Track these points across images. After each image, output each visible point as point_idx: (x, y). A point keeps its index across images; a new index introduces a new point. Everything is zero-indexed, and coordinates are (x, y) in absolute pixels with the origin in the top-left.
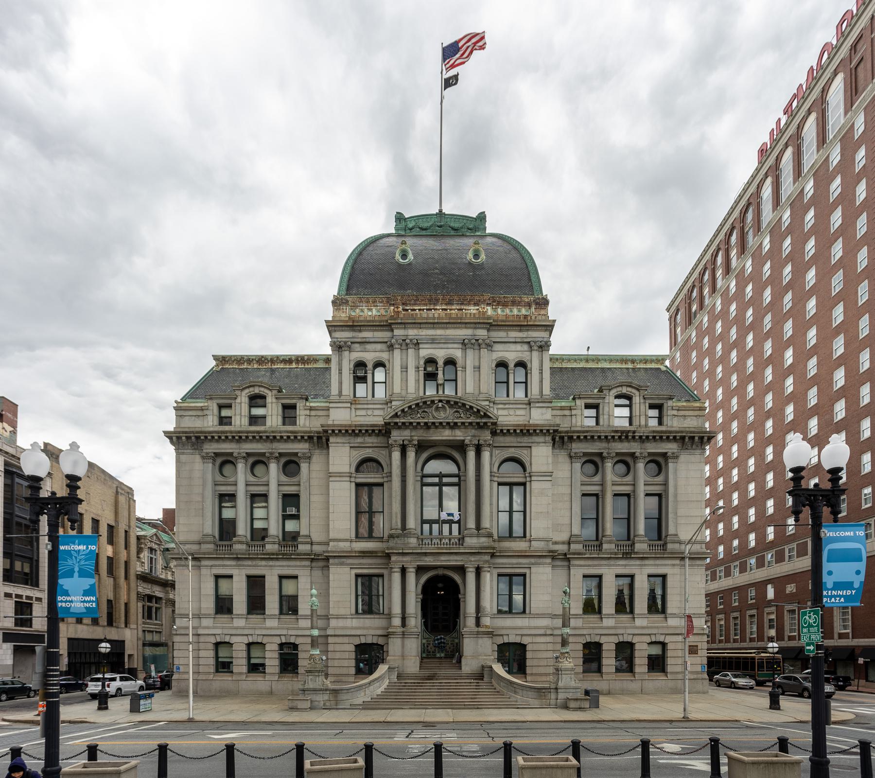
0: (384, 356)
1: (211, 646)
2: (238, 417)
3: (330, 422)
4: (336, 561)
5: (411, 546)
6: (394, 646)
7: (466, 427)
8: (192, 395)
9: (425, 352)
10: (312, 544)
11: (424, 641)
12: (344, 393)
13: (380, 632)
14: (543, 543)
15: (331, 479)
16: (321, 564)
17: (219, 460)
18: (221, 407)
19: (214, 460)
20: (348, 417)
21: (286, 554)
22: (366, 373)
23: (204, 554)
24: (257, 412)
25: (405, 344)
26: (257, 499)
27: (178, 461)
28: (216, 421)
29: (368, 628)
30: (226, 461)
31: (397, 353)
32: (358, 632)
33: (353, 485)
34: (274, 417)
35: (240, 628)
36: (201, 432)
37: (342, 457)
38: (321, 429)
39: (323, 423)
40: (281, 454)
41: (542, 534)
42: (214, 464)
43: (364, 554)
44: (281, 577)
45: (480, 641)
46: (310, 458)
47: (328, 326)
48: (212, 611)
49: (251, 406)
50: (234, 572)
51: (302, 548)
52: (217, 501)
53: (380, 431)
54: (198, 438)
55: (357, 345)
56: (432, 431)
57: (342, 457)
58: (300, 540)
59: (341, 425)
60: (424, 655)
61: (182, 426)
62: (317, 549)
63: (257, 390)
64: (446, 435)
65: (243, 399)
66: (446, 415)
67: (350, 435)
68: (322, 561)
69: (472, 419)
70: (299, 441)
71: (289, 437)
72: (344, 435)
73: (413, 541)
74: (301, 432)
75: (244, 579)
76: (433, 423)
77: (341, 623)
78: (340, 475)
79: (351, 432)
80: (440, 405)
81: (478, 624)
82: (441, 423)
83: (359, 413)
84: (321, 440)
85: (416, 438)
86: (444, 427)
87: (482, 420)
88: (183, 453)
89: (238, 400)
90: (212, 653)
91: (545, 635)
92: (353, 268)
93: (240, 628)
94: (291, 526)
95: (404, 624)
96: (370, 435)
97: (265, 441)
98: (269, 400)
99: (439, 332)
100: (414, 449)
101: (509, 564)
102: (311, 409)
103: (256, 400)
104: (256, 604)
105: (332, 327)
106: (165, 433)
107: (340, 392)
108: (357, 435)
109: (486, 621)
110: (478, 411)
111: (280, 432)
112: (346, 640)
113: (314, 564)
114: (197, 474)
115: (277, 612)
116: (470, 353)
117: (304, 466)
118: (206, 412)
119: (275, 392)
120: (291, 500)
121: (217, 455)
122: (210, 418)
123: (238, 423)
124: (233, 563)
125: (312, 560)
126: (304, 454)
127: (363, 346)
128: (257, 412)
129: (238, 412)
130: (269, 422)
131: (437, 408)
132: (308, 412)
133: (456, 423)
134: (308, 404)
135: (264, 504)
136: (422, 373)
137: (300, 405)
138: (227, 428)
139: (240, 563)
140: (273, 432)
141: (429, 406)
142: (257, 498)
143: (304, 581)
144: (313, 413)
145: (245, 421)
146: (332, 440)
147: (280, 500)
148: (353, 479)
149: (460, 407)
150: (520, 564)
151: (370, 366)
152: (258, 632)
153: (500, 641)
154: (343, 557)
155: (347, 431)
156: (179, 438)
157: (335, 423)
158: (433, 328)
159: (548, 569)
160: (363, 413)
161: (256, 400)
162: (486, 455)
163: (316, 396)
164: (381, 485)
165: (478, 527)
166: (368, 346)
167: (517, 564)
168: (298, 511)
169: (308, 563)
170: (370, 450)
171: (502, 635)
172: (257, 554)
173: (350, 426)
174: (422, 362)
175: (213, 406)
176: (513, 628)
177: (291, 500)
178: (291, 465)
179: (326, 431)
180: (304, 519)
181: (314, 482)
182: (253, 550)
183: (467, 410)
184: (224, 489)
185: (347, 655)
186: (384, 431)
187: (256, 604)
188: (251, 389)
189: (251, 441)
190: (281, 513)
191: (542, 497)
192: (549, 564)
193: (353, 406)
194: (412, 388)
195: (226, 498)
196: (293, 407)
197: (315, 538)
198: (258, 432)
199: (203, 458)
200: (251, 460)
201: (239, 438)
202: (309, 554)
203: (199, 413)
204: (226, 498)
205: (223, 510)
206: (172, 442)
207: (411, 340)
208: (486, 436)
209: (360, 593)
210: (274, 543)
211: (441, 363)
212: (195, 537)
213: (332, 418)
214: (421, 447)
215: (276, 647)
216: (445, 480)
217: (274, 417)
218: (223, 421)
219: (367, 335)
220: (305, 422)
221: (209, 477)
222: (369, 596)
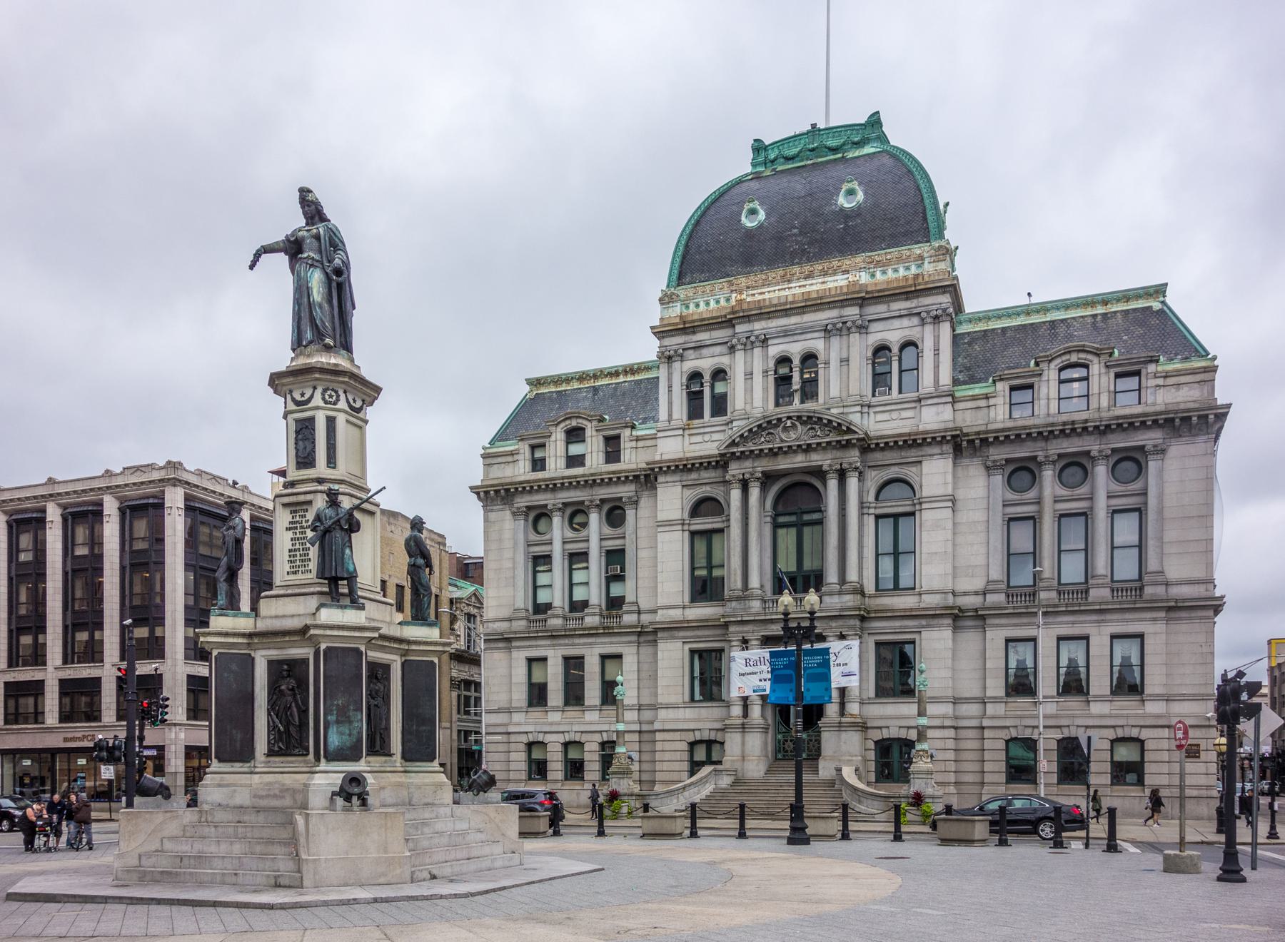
0: (724, 361)
1: (522, 747)
2: (553, 459)
3: (658, 458)
4: (665, 634)
5: (753, 610)
6: (733, 743)
7: (824, 449)
8: (501, 436)
9: (775, 350)
10: (639, 613)
11: (779, 737)
12: (675, 417)
13: (718, 725)
14: (938, 596)
15: (660, 529)
16: (650, 638)
17: (532, 516)
18: (533, 448)
19: (527, 515)
20: (680, 448)
21: (608, 628)
22: (702, 385)
23: (515, 633)
24: (575, 449)
25: (749, 344)
26: (575, 559)
27: (486, 520)
28: (528, 465)
29: (703, 719)
30: (539, 516)
31: (740, 355)
32: (692, 726)
33: (687, 534)
34: (594, 454)
35: (556, 724)
36: (511, 484)
37: (672, 500)
38: (644, 466)
39: (649, 459)
40: (603, 501)
41: (937, 584)
42: (526, 520)
43: (703, 624)
44: (604, 658)
45: (844, 735)
46: (636, 502)
47: (654, 333)
48: (524, 704)
49: (568, 443)
50: (549, 653)
51: (629, 619)
52: (530, 564)
53: (717, 462)
54: (507, 490)
55: (691, 352)
56: (780, 457)
57: (672, 500)
58: (625, 608)
59: (670, 461)
60: (780, 756)
61: (491, 476)
62: (646, 618)
63: (574, 423)
64: (798, 461)
65: (559, 435)
66: (798, 435)
67: (682, 471)
68: (648, 635)
69: (833, 437)
70: (624, 482)
71: (610, 479)
72: (674, 472)
73: (756, 605)
74: (625, 471)
75: (560, 661)
76: (780, 448)
77: (671, 714)
78: (669, 523)
79: (683, 468)
80: (789, 423)
81: (842, 712)
82: (790, 447)
83: (695, 439)
84: (648, 479)
85: (760, 469)
86: (795, 452)
87: (842, 436)
88: (492, 511)
89: (553, 438)
90: (523, 756)
91: (943, 727)
92: (687, 246)
93: (556, 724)
94: (616, 590)
95: (746, 714)
96: (706, 468)
97: (584, 486)
98: (589, 432)
99: (794, 320)
100: (757, 484)
101: (890, 628)
102: (638, 439)
103: (575, 435)
104: (574, 695)
105: (660, 333)
106: (471, 488)
107: (670, 415)
108: (690, 470)
109: (853, 708)
110: (839, 424)
111: (601, 474)
112: (677, 736)
113: (642, 639)
114: (507, 535)
115: (597, 702)
117: (630, 513)
118: (516, 457)
119: (595, 423)
120: (615, 557)
121: (529, 508)
122: (521, 464)
123: (553, 466)
124: (548, 642)
125: (640, 634)
126: (630, 498)
127: (698, 352)
128: (575, 449)
129: (552, 453)
130: (588, 462)
132: (633, 444)
133: (809, 445)
134: (634, 433)
135: (584, 565)
136: (771, 379)
137: (626, 433)
138: (540, 475)
139: (555, 642)
140: (592, 475)
141: (776, 426)
142: (577, 558)
143: (630, 662)
144: (641, 444)
145: (562, 462)
146: (660, 479)
147: (603, 559)
148: (686, 527)
149: (816, 423)
150: (906, 627)
151: (707, 377)
152: (576, 728)
153: (877, 735)
154: (672, 629)
155: (677, 466)
156: (487, 493)
157: (665, 457)
158: (786, 316)
159: (947, 633)
160: (699, 439)
161: (575, 435)
162: (853, 483)
163: (645, 421)
164: (721, 531)
165: (843, 580)
166: (705, 351)
167: (901, 627)
169: (634, 638)
170: (708, 488)
171: (880, 728)
172: (575, 630)
173: (680, 460)
174: (771, 364)
175: (524, 448)
176: (896, 716)
177: (615, 557)
178: (615, 514)
179: (653, 469)
180: (630, 583)
181: (641, 533)
182: (571, 624)
183: (826, 425)
184: (538, 550)
185: (678, 756)
186: (721, 462)
187: (574, 695)
188: (568, 422)
189: (568, 488)
190: (603, 575)
191: (932, 533)
192: (948, 625)
193: (687, 432)
194: (758, 402)
195: (541, 561)
196: (618, 437)
197: (644, 605)
198: (576, 477)
199: (514, 514)
200: (569, 511)
201: (553, 486)
202: (636, 627)
203: (510, 459)
204: (541, 561)
205: (539, 575)
206: (479, 498)
207: (757, 337)
208: (854, 456)
209: (697, 673)
210: (594, 614)
211: (796, 362)
212: (506, 613)
213: (660, 450)
214: (768, 479)
215: (596, 747)
216: (806, 517)
217: (594, 454)
218: (538, 464)
219: (703, 336)
220: (632, 459)
221: (521, 536)
222: (708, 677)
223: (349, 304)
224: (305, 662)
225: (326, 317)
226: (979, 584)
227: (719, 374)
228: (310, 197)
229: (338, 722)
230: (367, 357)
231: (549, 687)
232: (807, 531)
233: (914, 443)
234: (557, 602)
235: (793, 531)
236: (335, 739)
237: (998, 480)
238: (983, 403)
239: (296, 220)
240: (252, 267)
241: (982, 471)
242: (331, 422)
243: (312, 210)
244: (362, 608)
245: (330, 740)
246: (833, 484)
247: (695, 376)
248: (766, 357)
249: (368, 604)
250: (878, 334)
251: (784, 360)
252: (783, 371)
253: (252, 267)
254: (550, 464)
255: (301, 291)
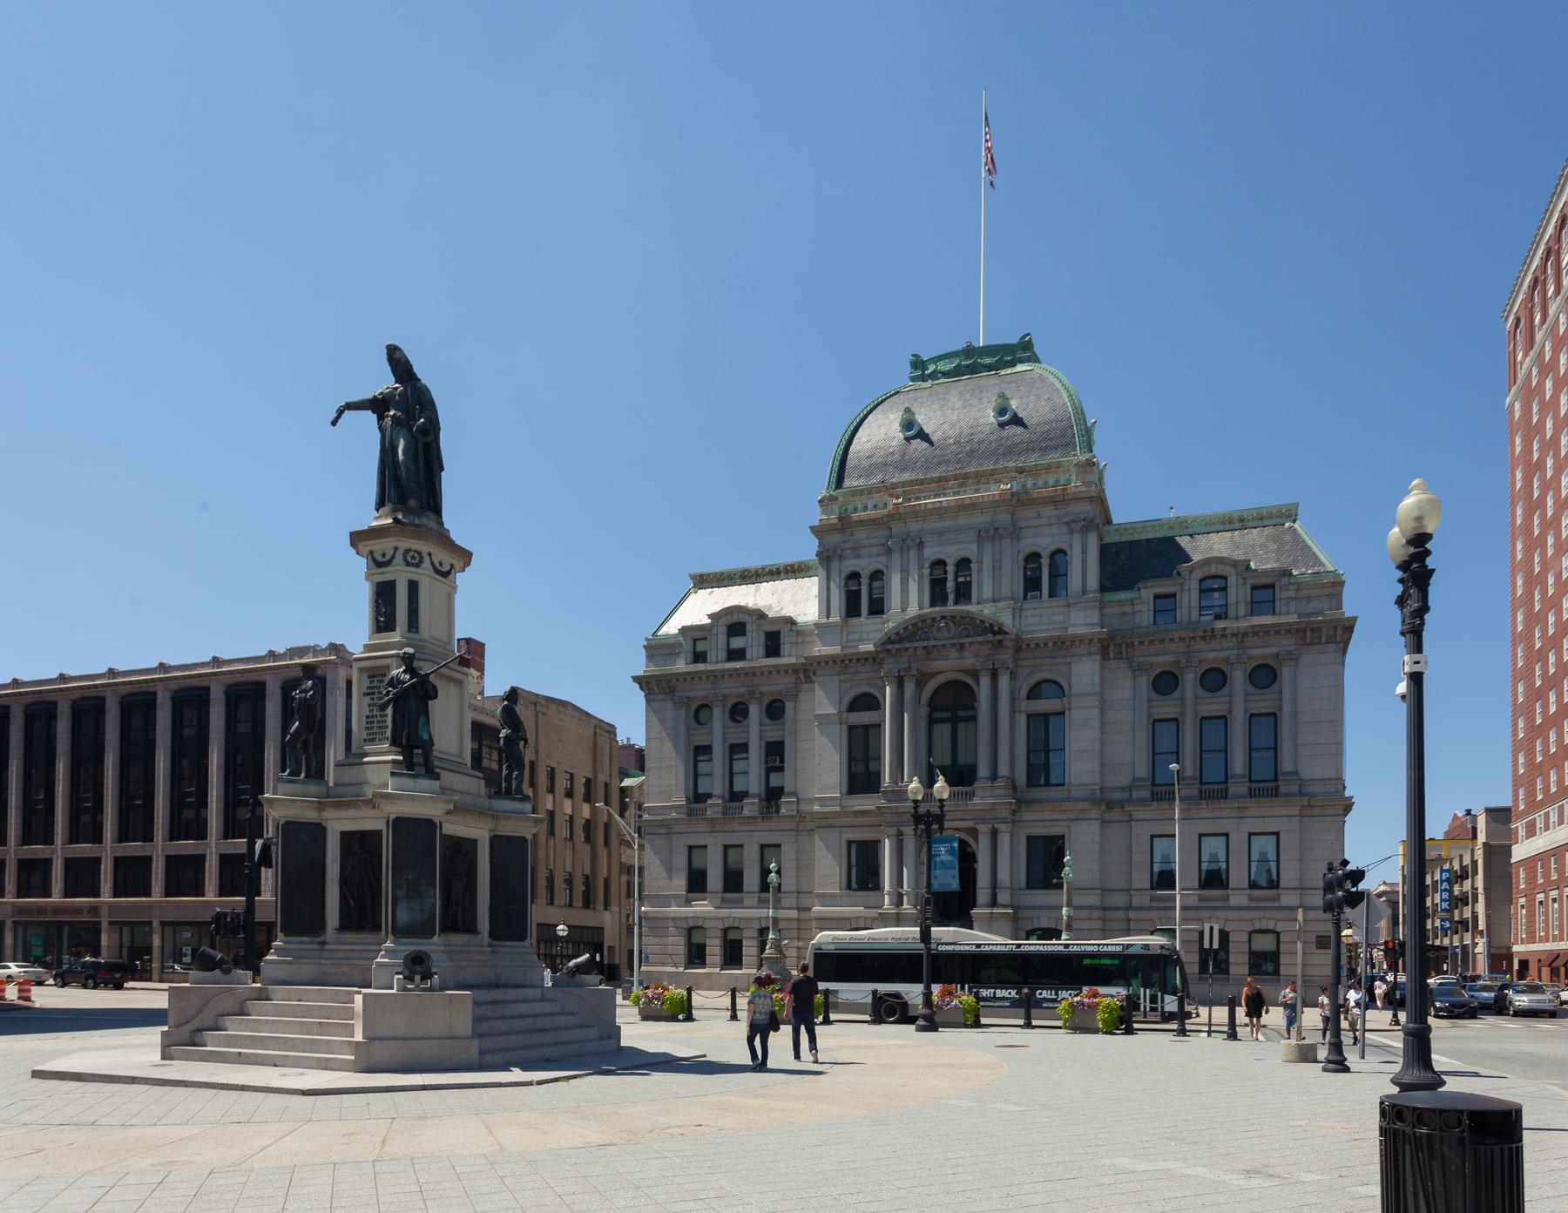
9: (931, 553)
24: (737, 642)
33: (844, 728)
90: (682, 940)
94: (775, 780)
104: (733, 881)
116: (988, 547)
117: (789, 706)
128: (737, 642)
130: (748, 656)
131: (939, 628)
132: (793, 639)
138: (701, 667)
142: (737, 749)
143: (788, 852)
145: (723, 655)
159: (1095, 827)
162: (1004, 682)
168: (782, 761)
177: (775, 752)
180: (788, 773)
205: (700, 765)
223: (435, 465)
224: (379, 833)
225: (412, 477)
226: (1124, 781)
227: (877, 575)
228: (397, 355)
229: (407, 897)
230: (457, 518)
231: (710, 873)
232: (961, 726)
233: (1063, 645)
234: (717, 790)
235: (947, 728)
236: (404, 916)
237: (1144, 682)
238: (1128, 609)
239: (384, 381)
240: (334, 423)
241: (1129, 672)
242: (413, 587)
243: (399, 363)
244: (437, 777)
245: (399, 916)
246: (985, 681)
247: (855, 576)
248: (921, 559)
249: (444, 774)
250: (1030, 543)
251: (940, 563)
252: (938, 573)
253: (334, 423)
254: (711, 656)
255: (387, 452)
